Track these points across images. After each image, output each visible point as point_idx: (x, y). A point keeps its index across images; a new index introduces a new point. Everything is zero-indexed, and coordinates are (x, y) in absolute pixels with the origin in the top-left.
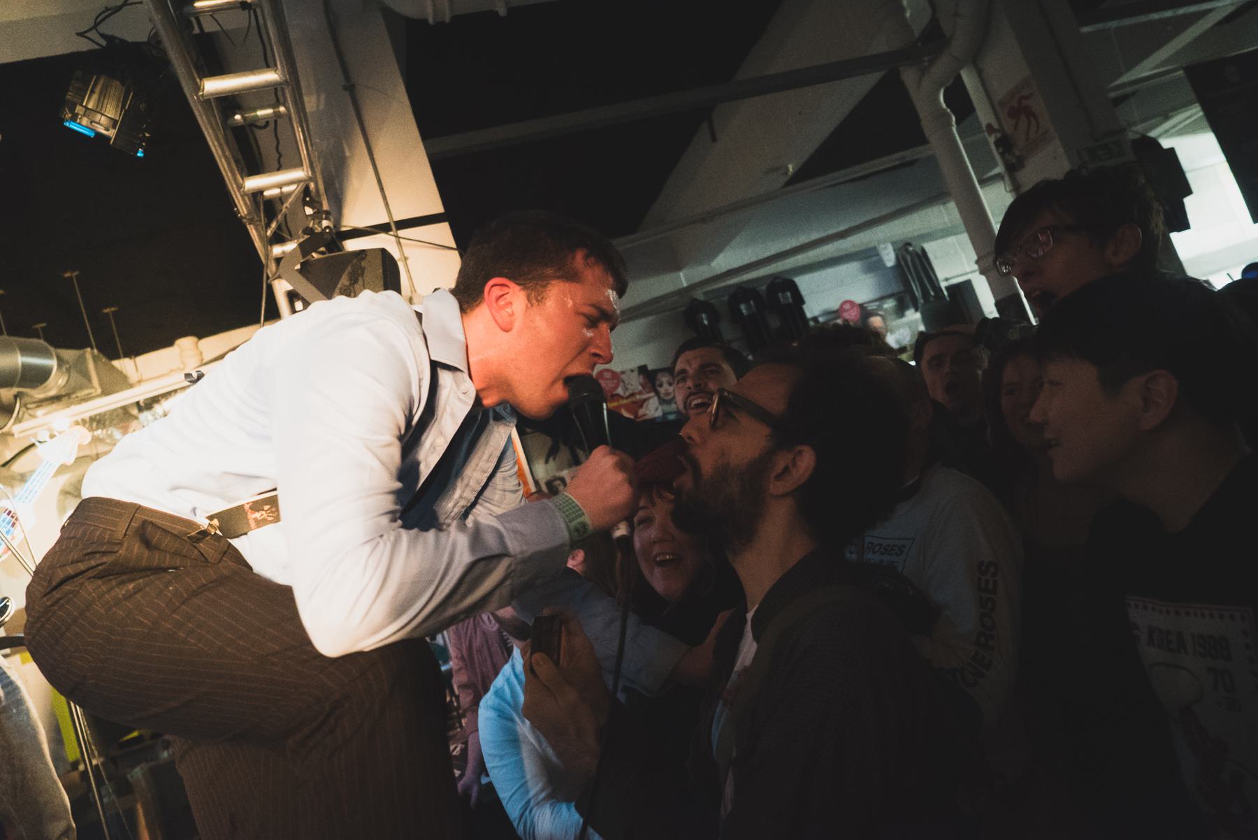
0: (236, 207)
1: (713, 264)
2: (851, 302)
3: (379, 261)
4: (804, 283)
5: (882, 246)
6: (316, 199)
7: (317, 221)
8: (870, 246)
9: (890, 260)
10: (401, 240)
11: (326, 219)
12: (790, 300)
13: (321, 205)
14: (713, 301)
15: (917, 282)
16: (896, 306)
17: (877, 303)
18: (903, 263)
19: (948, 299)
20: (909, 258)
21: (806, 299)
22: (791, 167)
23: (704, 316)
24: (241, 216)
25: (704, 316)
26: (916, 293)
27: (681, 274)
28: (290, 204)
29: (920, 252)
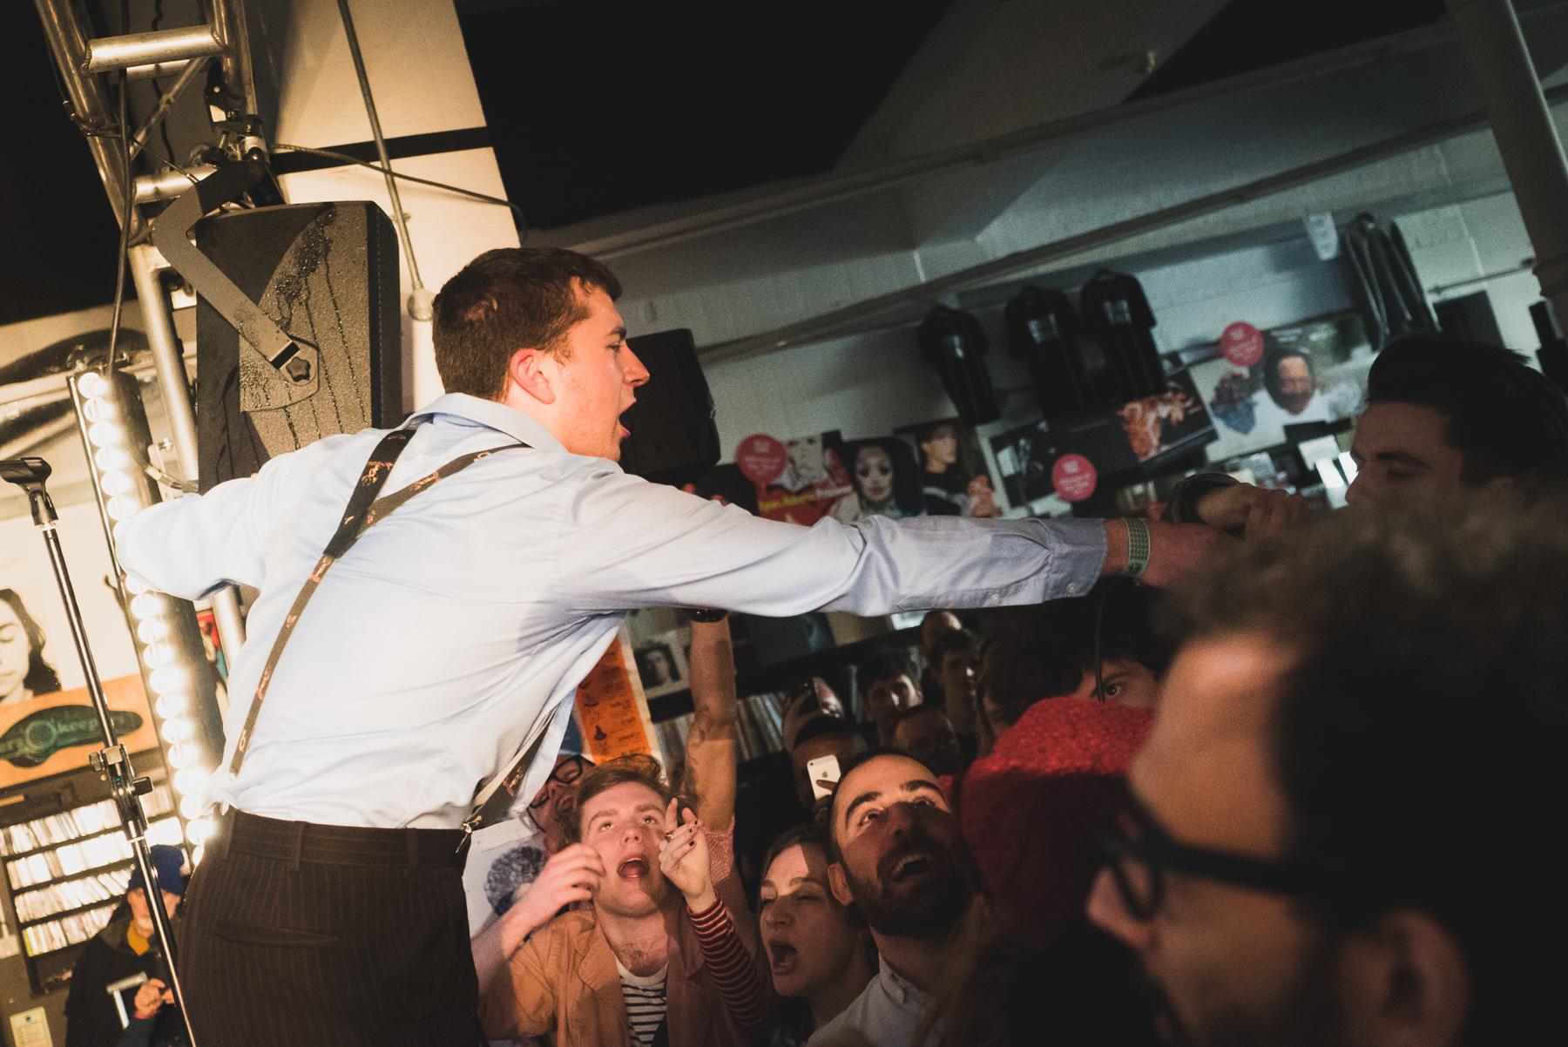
0: (68, 97)
1: (979, 239)
2: (1247, 328)
3: (361, 227)
4: (1156, 284)
5: (1313, 218)
6: (236, 91)
7: (234, 136)
8: (1291, 216)
9: (1326, 247)
10: (397, 179)
11: (252, 134)
12: (1128, 316)
13: (245, 104)
14: (973, 312)
15: (1380, 296)
16: (1334, 338)
17: (1298, 331)
18: (1353, 255)
19: (1439, 328)
20: (1365, 244)
21: (1157, 315)
22: (1152, 58)
23: (957, 340)
24: (77, 116)
25: (957, 340)
26: (1377, 315)
27: (916, 256)
28: (175, 96)
29: (1387, 233)
